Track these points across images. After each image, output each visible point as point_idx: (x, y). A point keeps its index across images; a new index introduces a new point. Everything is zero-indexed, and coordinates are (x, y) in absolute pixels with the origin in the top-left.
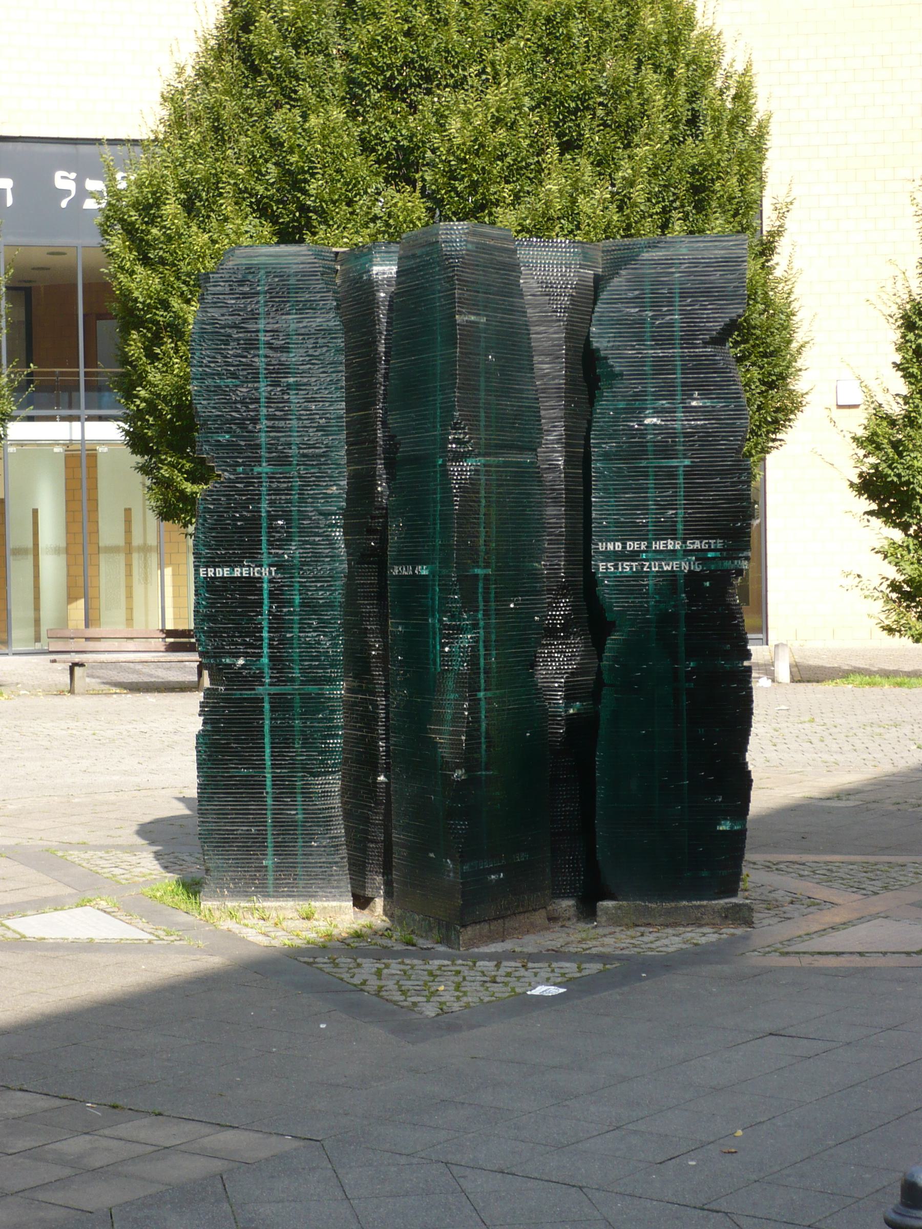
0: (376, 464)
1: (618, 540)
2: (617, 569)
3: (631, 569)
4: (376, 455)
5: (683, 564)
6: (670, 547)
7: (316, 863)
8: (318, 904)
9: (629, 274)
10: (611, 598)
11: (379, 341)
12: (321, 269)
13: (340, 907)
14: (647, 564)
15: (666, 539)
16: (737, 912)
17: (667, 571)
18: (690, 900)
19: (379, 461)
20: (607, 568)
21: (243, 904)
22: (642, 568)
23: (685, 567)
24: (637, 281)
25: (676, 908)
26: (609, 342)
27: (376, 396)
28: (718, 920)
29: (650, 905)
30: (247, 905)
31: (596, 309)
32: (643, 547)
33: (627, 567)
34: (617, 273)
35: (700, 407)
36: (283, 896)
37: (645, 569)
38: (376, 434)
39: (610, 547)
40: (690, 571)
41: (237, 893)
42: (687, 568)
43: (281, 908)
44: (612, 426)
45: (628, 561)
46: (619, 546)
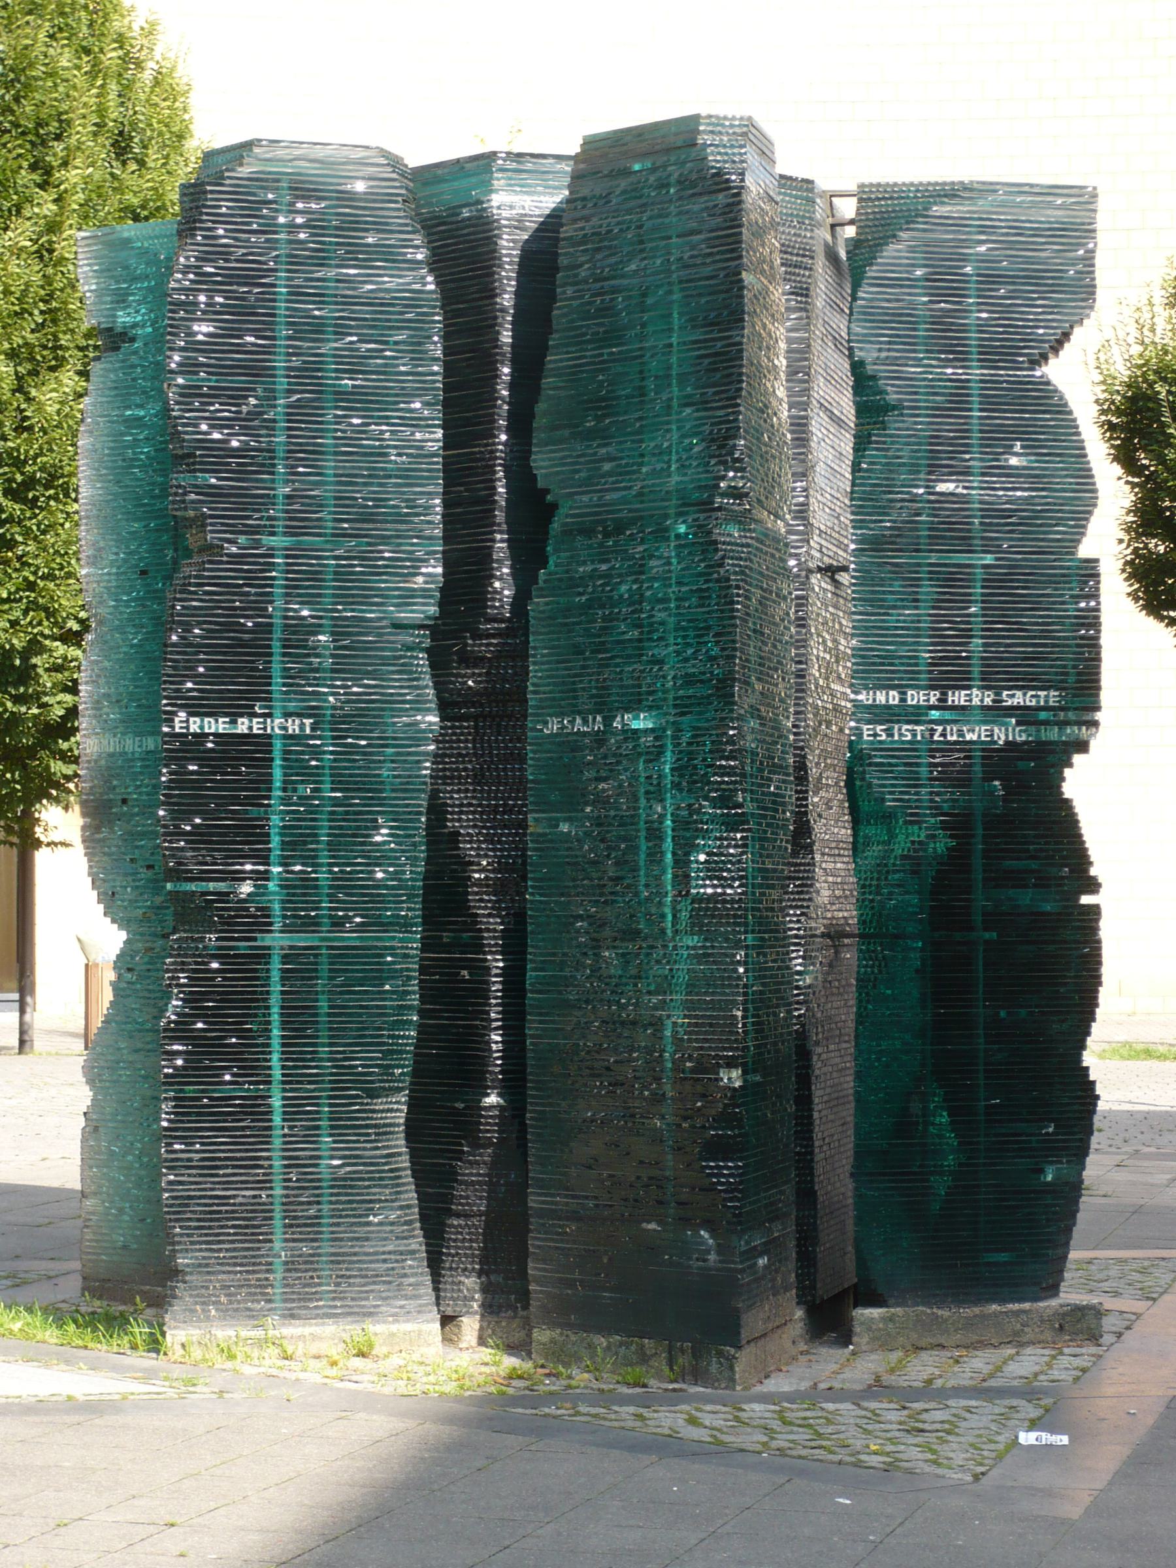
0: (494, 541)
1: (893, 687)
2: (892, 735)
3: (915, 735)
4: (494, 524)
5: (996, 730)
6: (976, 701)
7: (376, 1253)
8: (380, 1328)
9: (913, 239)
10: (884, 786)
11: (501, 325)
12: (403, 191)
13: (420, 1333)
14: (940, 728)
15: (969, 687)
16: (1079, 1321)
17: (971, 742)
18: (1003, 1301)
19: (498, 537)
20: (875, 735)
21: (244, 1333)
22: (932, 735)
23: (1000, 736)
24: (929, 253)
25: (983, 1316)
26: (880, 350)
27: (495, 421)
28: (1048, 1335)
29: (940, 1312)
30: (252, 1334)
31: (860, 294)
32: (933, 700)
33: (906, 732)
34: (894, 236)
35: (1024, 468)
36: (317, 1317)
37: (936, 738)
38: (494, 488)
39: (881, 697)
40: (1007, 743)
41: (231, 1313)
42: (1003, 737)
43: (314, 1337)
44: (885, 492)
45: (908, 722)
46: (894, 697)
